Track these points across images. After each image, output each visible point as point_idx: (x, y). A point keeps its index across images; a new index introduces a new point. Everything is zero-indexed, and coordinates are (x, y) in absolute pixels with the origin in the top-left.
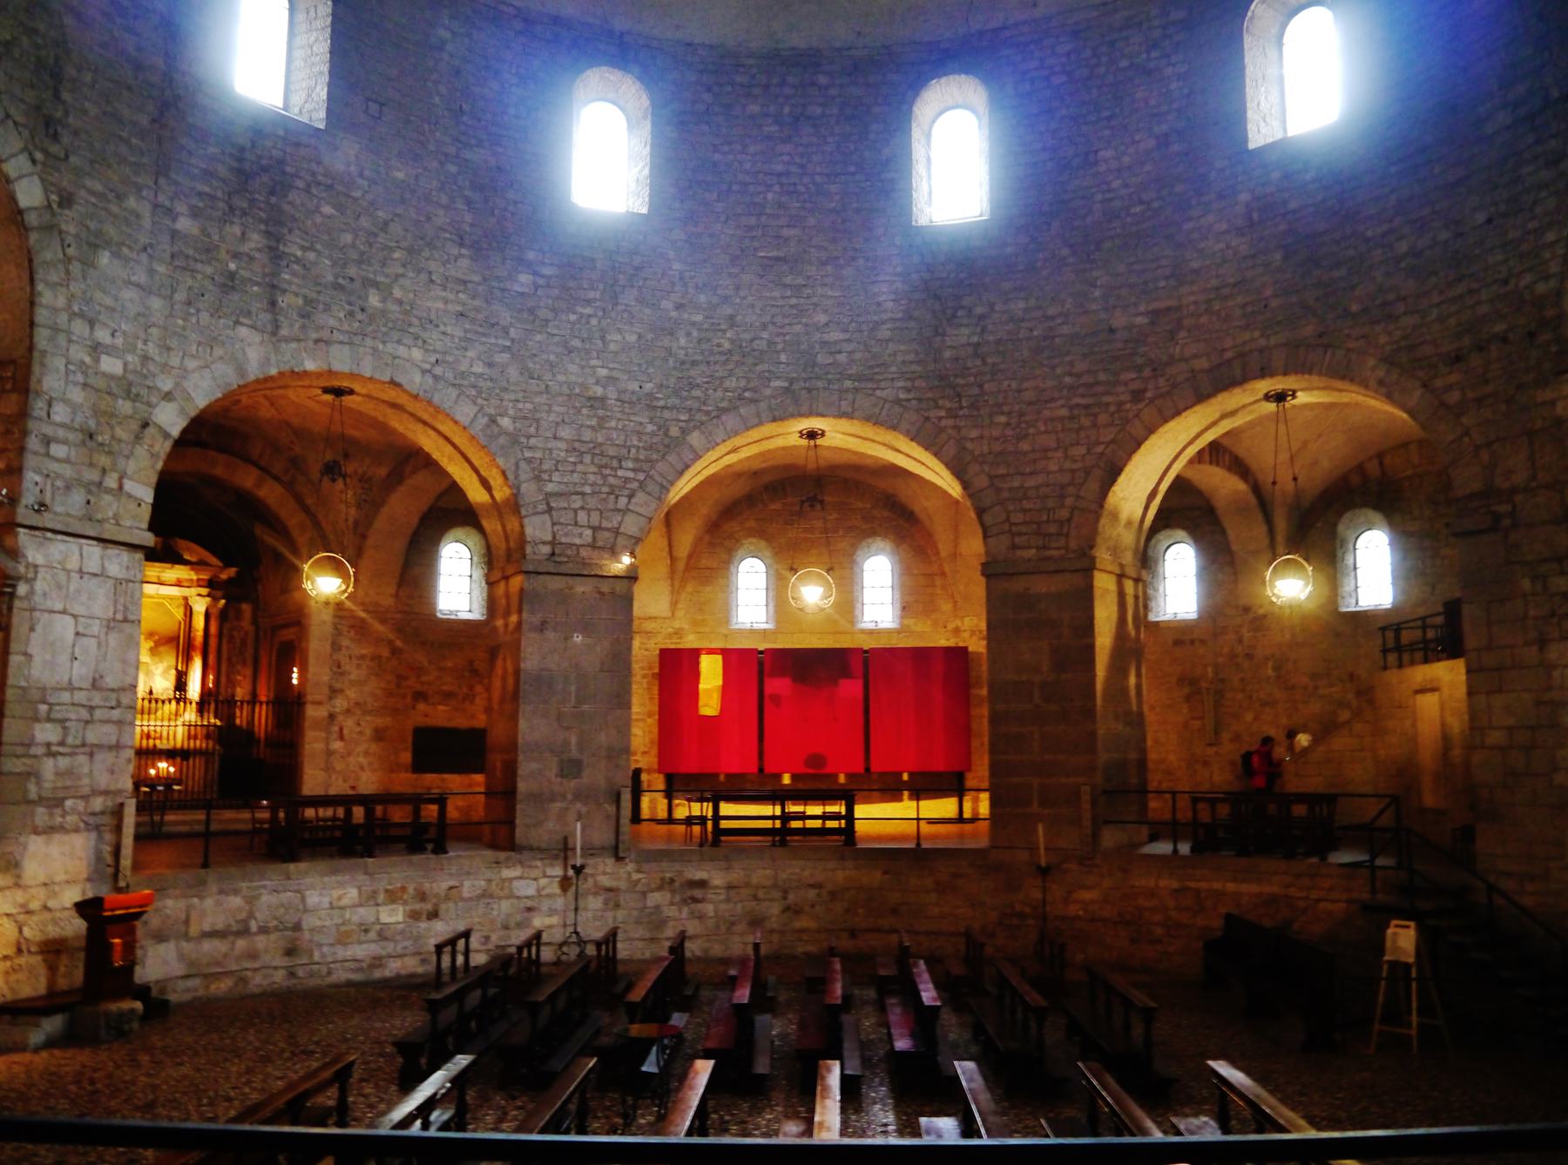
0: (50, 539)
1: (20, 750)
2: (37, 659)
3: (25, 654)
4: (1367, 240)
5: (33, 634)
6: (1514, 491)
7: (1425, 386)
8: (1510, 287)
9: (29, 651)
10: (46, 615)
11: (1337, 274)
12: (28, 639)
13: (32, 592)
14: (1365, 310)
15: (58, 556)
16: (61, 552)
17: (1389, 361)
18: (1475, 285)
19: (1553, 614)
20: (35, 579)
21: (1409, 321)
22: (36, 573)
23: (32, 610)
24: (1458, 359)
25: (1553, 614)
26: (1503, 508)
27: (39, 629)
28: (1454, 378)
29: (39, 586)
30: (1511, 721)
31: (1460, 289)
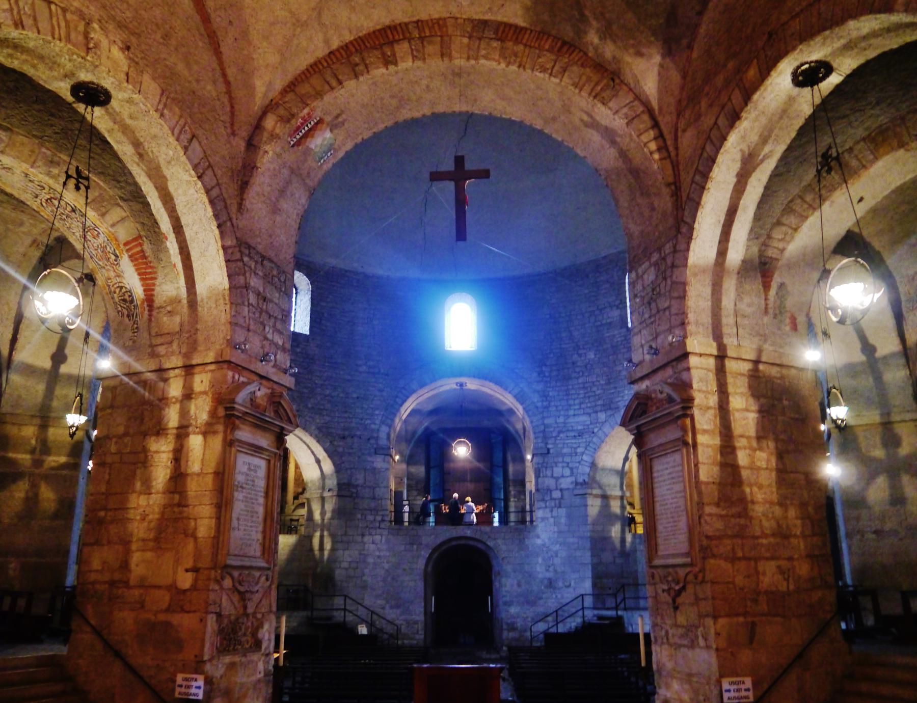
4: (316, 384)
6: (357, 486)
7: (331, 442)
8: (363, 422)
11: (305, 390)
14: (313, 408)
17: (319, 429)
18: (351, 416)
19: (367, 527)
21: (328, 418)
24: (344, 438)
25: (367, 527)
26: (354, 490)
28: (341, 443)
30: (349, 559)
31: (346, 415)
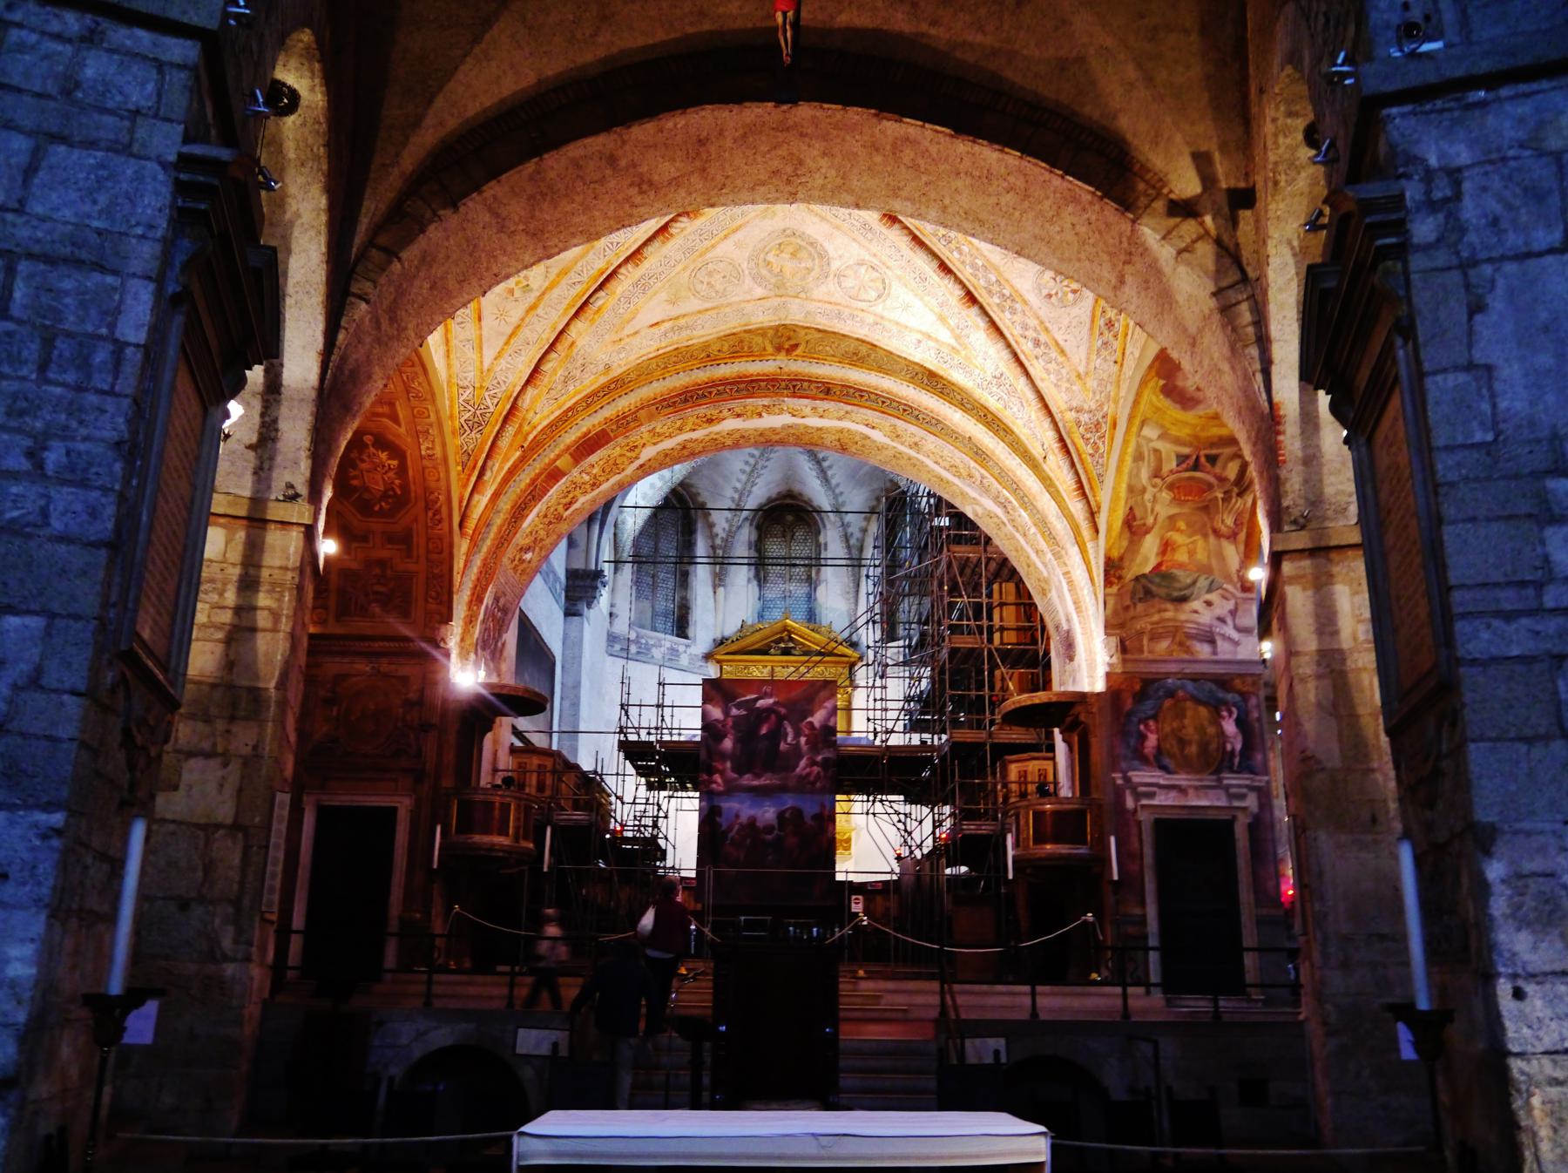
0: (1482, 104)
1: (1508, 599)
2: (1510, 372)
3: (1470, 367)
5: (1478, 318)
9: (1479, 356)
10: (1510, 268)
12: (1470, 332)
13: (1455, 228)
15: (1510, 132)
16: (1521, 121)
20: (1458, 196)
22: (1457, 185)
23: (1466, 265)
27: (1497, 303)
29: (1469, 210)
